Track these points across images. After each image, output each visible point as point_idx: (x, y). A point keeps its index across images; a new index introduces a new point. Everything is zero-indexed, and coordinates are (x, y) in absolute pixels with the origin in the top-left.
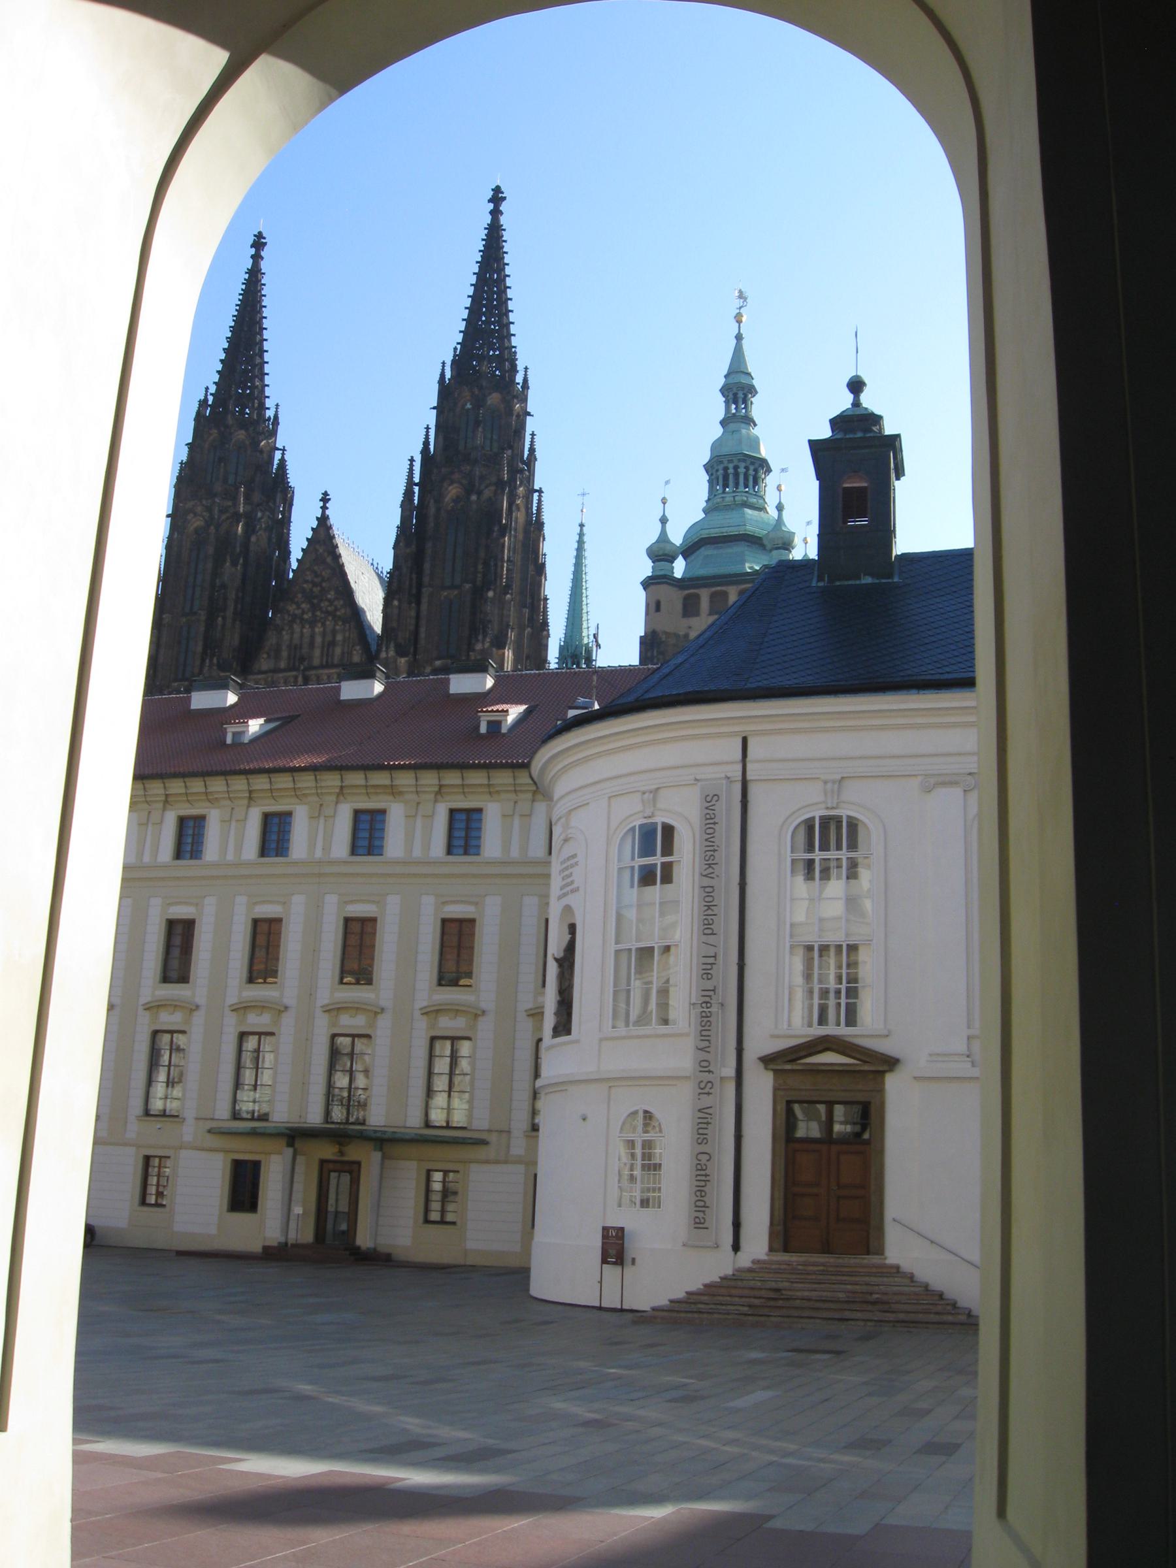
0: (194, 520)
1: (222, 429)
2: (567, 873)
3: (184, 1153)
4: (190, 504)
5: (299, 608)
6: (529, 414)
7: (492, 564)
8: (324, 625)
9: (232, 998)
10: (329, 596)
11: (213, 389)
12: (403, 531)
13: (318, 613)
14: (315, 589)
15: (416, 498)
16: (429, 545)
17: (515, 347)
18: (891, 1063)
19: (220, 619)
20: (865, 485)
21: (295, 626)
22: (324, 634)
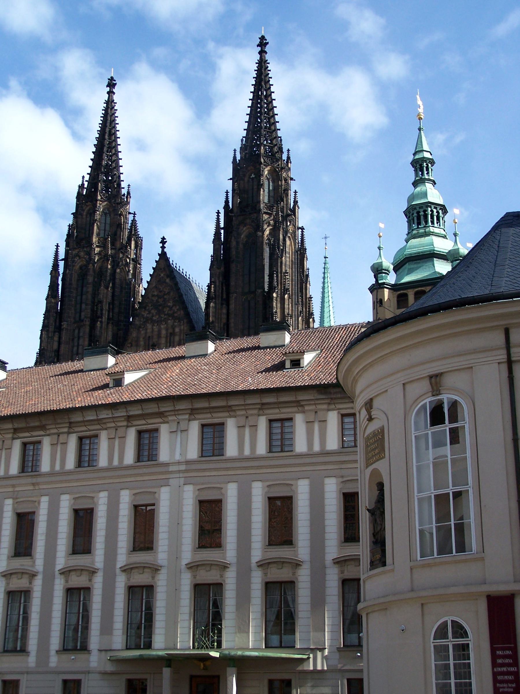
0: (79, 261)
1: (95, 202)
4: (75, 252)
5: (150, 312)
7: (275, 275)
10: (169, 304)
11: (87, 178)
13: (163, 316)
14: (160, 300)
15: (222, 237)
16: (233, 267)
17: (280, 137)
19: (99, 323)
21: (148, 325)
22: (167, 330)
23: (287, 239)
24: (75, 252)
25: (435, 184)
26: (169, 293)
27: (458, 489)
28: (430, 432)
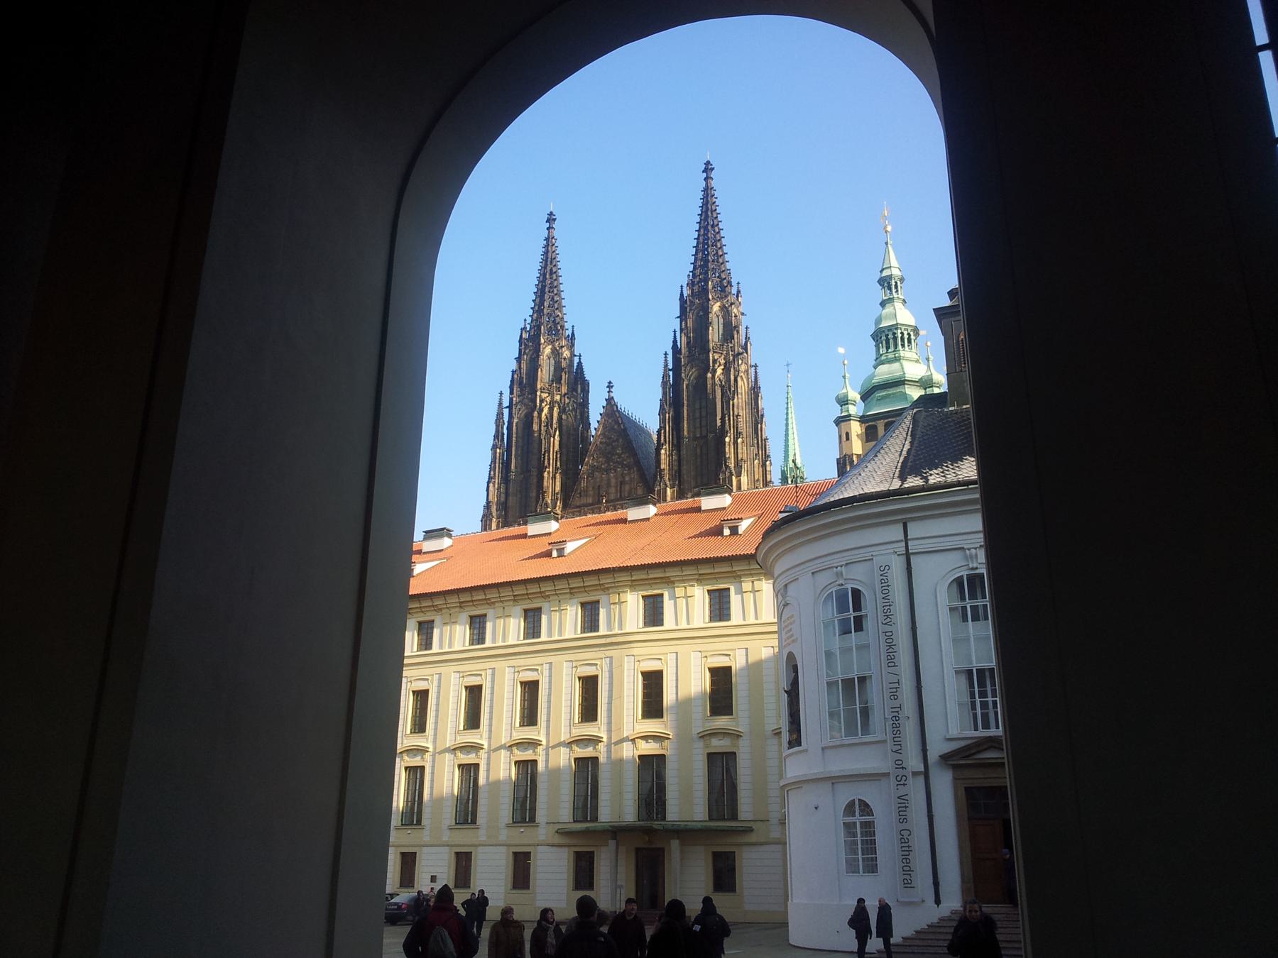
3: (540, 849)
7: (727, 418)
8: (616, 471)
13: (611, 464)
17: (729, 270)
19: (546, 473)
22: (616, 479)
23: (739, 379)
25: (906, 302)
26: (617, 440)
27: (861, 674)
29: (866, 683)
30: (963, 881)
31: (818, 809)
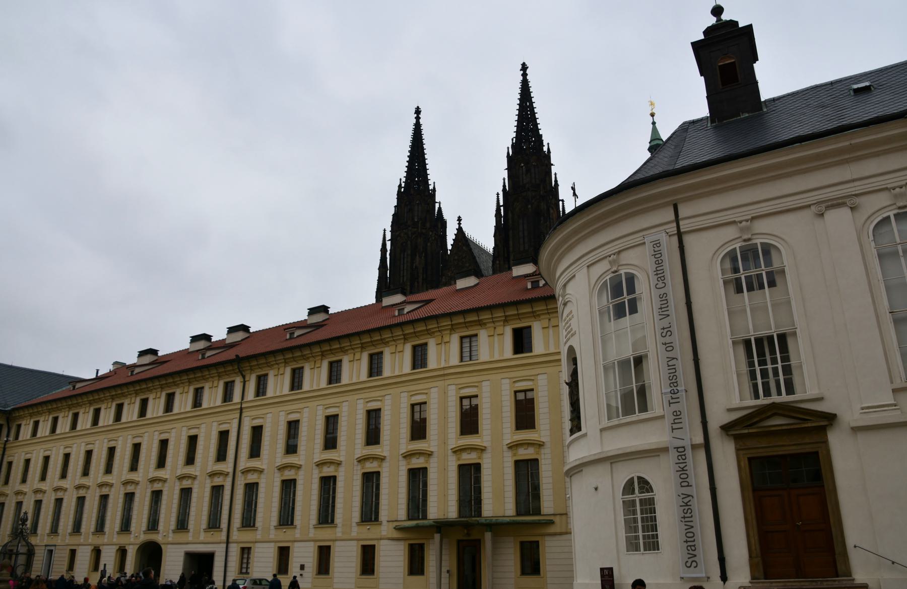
2: (568, 325)
3: (382, 542)
4: (397, 233)
6: (552, 165)
9: (403, 449)
11: (404, 180)
12: (497, 228)
16: (511, 232)
18: (830, 418)
20: (733, 61)
24: (397, 233)
28: (611, 306)
29: (642, 365)
30: (750, 557)
31: (599, 489)
